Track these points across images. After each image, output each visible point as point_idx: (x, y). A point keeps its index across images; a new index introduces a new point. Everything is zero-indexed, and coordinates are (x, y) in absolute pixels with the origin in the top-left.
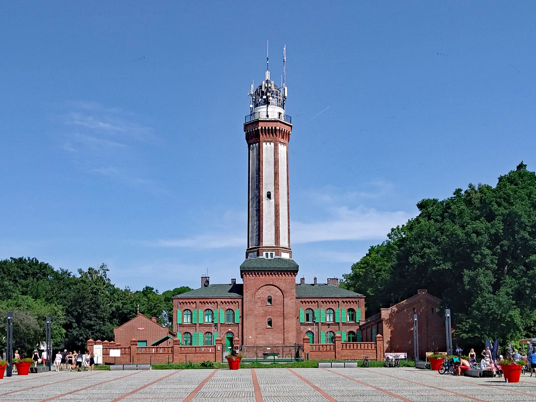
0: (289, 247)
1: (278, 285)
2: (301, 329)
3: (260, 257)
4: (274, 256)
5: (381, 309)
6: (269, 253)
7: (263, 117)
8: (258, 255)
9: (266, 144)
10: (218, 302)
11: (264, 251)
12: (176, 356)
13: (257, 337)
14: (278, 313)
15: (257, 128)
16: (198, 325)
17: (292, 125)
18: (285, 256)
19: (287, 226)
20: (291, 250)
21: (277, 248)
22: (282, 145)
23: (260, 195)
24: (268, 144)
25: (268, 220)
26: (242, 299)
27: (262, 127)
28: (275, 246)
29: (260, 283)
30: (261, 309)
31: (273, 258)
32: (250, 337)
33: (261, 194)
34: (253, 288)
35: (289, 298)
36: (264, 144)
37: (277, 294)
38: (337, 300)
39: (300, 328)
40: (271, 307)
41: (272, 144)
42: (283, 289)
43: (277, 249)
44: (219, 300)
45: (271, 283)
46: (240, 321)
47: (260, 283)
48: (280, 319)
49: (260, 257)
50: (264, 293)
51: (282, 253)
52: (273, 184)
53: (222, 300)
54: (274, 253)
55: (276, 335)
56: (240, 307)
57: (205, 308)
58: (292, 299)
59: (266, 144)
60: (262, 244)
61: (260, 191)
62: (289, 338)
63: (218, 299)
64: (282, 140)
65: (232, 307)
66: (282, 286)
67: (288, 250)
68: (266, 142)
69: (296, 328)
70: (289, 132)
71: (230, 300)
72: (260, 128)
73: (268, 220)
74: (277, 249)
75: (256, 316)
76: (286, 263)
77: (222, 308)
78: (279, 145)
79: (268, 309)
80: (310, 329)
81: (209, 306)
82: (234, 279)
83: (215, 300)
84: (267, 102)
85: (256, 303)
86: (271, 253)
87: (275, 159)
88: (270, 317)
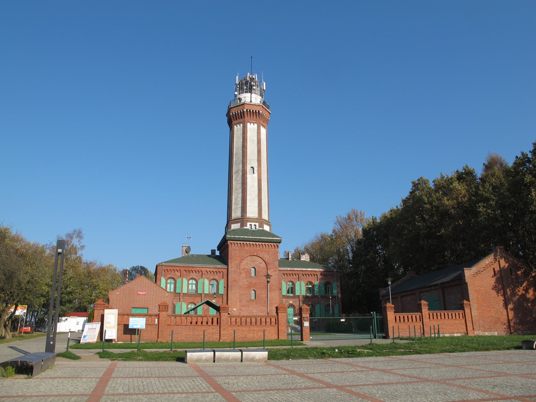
0: (269, 220)
1: (262, 256)
2: (283, 302)
3: (245, 228)
4: (257, 227)
5: (464, 269)
6: (253, 224)
7: (248, 100)
8: (242, 225)
9: (250, 125)
10: (203, 272)
11: (247, 222)
12: (224, 330)
13: (241, 310)
14: (262, 285)
15: (243, 110)
16: (182, 295)
17: (271, 112)
18: (266, 228)
19: (267, 200)
20: (270, 224)
21: (261, 220)
22: (263, 127)
23: (244, 169)
24: (252, 124)
25: (252, 193)
26: (228, 269)
27: (247, 110)
28: (258, 218)
29: (244, 254)
30: (245, 280)
31: (257, 230)
32: (235, 309)
33: (245, 168)
34: (238, 258)
35: (272, 270)
36: (248, 124)
37: (261, 265)
38: (316, 273)
39: (282, 301)
40: (255, 279)
41: (256, 125)
42: (266, 260)
43: (260, 220)
44: (204, 269)
45: (255, 254)
46: (224, 292)
47: (244, 254)
48: (264, 291)
49: (245, 228)
50: (248, 263)
51: (265, 226)
52: (256, 160)
53: (206, 269)
54: (257, 224)
55: (260, 307)
56: (225, 277)
57: (190, 277)
58: (275, 271)
59: (250, 125)
60: (246, 216)
61: (244, 166)
62: (272, 311)
63: (203, 269)
64: (263, 123)
65: (217, 277)
66: (266, 257)
67: (268, 223)
68: (250, 123)
69: (279, 300)
70: (268, 118)
71: (214, 270)
72: (245, 110)
73: (252, 193)
74: (260, 220)
75: (240, 287)
76: (270, 235)
77: (207, 278)
78: (261, 126)
79: (252, 281)
80: (291, 302)
81: (194, 275)
82: (213, 250)
83: (200, 269)
84: (250, 90)
85: (241, 274)
86: (254, 225)
87: (258, 138)
88: (254, 289)
